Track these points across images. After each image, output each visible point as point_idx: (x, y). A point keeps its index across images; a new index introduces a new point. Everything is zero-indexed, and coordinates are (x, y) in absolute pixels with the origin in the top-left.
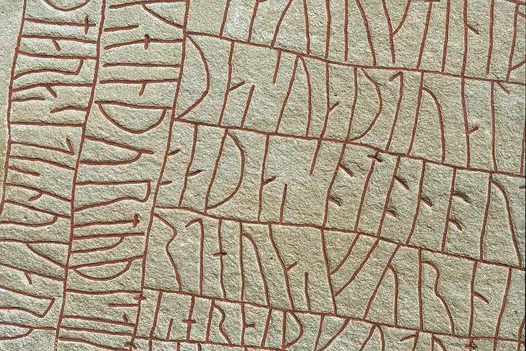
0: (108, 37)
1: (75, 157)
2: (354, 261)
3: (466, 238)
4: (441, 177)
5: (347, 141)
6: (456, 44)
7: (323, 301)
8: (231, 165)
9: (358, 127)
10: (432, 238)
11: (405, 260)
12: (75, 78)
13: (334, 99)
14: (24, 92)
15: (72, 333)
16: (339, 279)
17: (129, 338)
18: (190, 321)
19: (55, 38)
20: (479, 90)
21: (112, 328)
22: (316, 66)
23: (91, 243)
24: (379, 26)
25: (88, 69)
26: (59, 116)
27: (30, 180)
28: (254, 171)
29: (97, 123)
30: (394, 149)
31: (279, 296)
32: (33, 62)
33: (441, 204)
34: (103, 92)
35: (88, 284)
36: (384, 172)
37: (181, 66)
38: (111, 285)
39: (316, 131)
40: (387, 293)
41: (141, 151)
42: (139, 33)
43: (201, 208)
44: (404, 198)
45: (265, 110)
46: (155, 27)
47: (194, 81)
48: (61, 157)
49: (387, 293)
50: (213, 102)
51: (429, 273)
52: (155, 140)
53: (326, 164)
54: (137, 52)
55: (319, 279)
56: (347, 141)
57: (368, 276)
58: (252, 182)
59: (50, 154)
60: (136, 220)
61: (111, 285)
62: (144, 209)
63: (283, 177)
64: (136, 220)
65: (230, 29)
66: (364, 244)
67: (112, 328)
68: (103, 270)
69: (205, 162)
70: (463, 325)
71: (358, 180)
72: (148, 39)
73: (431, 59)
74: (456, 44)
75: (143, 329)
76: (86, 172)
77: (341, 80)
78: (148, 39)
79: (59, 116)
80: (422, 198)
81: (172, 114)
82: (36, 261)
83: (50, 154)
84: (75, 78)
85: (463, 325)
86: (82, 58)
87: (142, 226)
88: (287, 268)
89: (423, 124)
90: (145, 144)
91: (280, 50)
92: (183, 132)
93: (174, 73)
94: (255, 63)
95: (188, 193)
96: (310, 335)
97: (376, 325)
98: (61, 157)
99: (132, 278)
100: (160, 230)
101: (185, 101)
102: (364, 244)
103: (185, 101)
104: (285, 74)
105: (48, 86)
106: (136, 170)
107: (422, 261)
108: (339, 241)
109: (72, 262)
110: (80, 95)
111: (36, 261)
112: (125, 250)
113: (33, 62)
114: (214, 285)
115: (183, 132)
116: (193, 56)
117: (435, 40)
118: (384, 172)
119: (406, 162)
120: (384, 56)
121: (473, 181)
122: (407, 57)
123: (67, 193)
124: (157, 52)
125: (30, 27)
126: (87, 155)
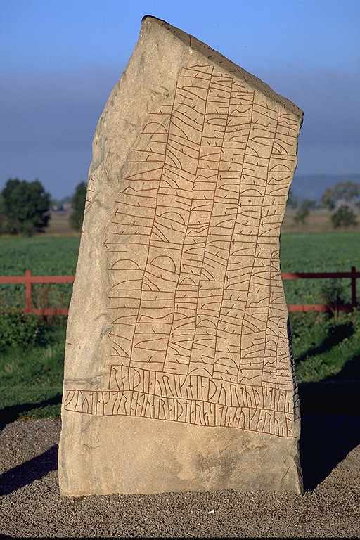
2: (251, 326)
6: (189, 300)
7: (262, 334)
8: (225, 362)
9: (213, 326)
10: (243, 304)
11: (249, 312)
13: (205, 333)
15: (276, 407)
16: (256, 330)
18: (271, 372)
19: (191, 413)
20: (202, 294)
21: (273, 395)
24: (185, 321)
25: (198, 403)
26: (213, 411)
28: (226, 355)
29: (215, 400)
32: (198, 419)
33: (233, 302)
34: (205, 399)
35: (261, 402)
40: (259, 317)
44: (232, 313)
45: (209, 352)
47: (201, 373)
48: (224, 411)
49: (259, 317)
50: (207, 367)
52: (219, 383)
54: (194, 389)
58: (229, 355)
59: (224, 414)
60: (242, 388)
65: (187, 363)
66: (245, 323)
67: (273, 395)
68: (257, 398)
70: (267, 295)
71: (227, 325)
72: (190, 386)
74: (189, 300)
75: (273, 386)
76: (229, 403)
77: (199, 331)
78: (190, 386)
79: (213, 411)
82: (255, 418)
83: (224, 414)
85: (267, 295)
88: (254, 345)
92: (216, 375)
94: (196, 355)
95: (233, 373)
96: (272, 338)
98: (224, 411)
101: (208, 375)
102: (245, 323)
103: (208, 375)
104: (198, 347)
106: (227, 388)
108: (245, 330)
111: (255, 418)
112: (250, 390)
113: (198, 419)
114: (259, 366)
115: (216, 375)
123: (235, 409)
126: (224, 404)
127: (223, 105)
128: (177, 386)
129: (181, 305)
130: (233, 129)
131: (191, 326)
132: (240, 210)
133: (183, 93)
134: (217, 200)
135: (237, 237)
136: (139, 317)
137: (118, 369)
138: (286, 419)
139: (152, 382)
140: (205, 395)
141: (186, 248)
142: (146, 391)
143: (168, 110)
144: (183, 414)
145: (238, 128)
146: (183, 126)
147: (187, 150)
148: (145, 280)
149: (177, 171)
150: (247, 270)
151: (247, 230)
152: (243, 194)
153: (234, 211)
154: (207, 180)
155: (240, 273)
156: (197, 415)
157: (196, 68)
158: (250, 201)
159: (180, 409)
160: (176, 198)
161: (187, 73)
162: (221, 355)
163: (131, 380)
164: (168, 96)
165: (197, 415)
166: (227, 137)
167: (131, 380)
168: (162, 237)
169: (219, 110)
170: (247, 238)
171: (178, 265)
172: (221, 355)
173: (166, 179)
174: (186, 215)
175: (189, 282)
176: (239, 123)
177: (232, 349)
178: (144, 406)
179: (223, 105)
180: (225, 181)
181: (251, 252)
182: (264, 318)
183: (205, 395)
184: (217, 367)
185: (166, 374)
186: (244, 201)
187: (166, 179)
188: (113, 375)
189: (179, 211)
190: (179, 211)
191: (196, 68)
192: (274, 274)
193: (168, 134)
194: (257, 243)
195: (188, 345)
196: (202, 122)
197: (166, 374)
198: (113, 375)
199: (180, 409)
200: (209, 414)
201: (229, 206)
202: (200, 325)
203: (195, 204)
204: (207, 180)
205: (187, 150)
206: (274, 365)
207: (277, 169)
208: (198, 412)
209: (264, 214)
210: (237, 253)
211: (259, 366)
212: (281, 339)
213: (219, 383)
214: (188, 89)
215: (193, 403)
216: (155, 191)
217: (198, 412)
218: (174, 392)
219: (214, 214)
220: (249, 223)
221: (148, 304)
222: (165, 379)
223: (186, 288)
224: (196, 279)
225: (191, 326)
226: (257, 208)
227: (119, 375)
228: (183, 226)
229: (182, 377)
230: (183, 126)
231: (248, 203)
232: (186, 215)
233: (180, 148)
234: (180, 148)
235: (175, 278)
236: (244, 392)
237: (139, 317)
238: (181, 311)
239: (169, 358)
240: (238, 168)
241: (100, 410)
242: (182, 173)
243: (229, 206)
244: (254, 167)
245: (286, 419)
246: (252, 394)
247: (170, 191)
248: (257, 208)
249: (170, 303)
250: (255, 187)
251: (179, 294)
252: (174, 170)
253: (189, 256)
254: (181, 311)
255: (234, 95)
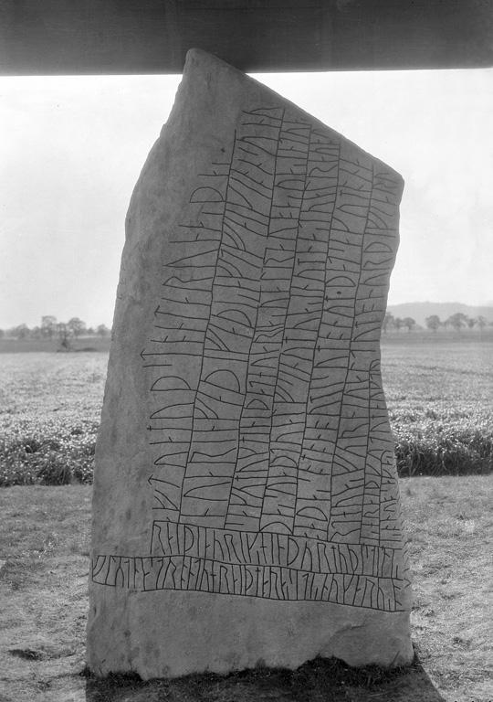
0: (262, 562)
1: (310, 574)
3: (334, 422)
4: (309, 433)
5: (297, 468)
6: (261, 430)
7: (360, 474)
9: (292, 464)
11: (343, 443)
12: (279, 575)
14: (286, 595)
16: (351, 468)
17: (380, 549)
18: (372, 525)
21: (376, 556)
22: (271, 481)
23: (344, 563)
24: (253, 459)
25: (274, 569)
27: (320, 590)
30: (300, 451)
31: (361, 490)
36: (309, 454)
37: (272, 533)
38: (360, 557)
39: (294, 480)
41: (306, 547)
42: (260, 550)
43: (327, 523)
45: (289, 500)
46: (258, 544)
47: (276, 528)
48: (310, 579)
51: (346, 435)
52: (301, 542)
53: (307, 476)
55: (352, 476)
56: (297, 468)
57: (348, 456)
59: (309, 584)
61: (360, 557)
62: (329, 545)
63: (314, 492)
64: (333, 548)
65: (258, 515)
67: (376, 556)
69: (310, 522)
73: (266, 439)
77: (273, 472)
79: (294, 581)
80: (318, 439)
81: (291, 536)
84: (279, 575)
86: (271, 572)
87: (336, 546)
89: (290, 440)
90: (304, 546)
91: (265, 496)
92: (298, 532)
93: (275, 535)
94: (270, 505)
97: (367, 453)
98: (310, 579)
99: (357, 549)
100: (338, 539)
101: (287, 531)
103: (287, 531)
105: (282, 585)
106: (313, 549)
107: (342, 437)
108: (338, 469)
109: (352, 572)
110: (285, 572)
111: (352, 589)
112: (343, 549)
113: (273, 591)
116: (268, 529)
117: (260, 438)
118: (309, 454)
119: (304, 446)
120: (266, 456)
121: (311, 420)
122: (265, 448)
124: (267, 543)
125: (260, 593)
127: (299, 162)
128: (245, 548)
129: (248, 437)
130: (313, 194)
131: (264, 465)
132: (328, 305)
133: (245, 146)
134: (294, 291)
135: (321, 343)
136: (191, 454)
137: (164, 525)
138: (394, 587)
139: (210, 541)
140: (283, 558)
141: (253, 359)
142: (202, 555)
143: (225, 170)
144: (254, 586)
145: (320, 192)
146: (245, 191)
147: (251, 224)
148: (198, 404)
149: (239, 253)
150: (340, 387)
151: (336, 332)
152: (330, 283)
153: (320, 306)
154: (280, 265)
155: (330, 390)
156: (273, 586)
157: (261, 112)
158: (339, 293)
159: (249, 580)
160: (238, 291)
161: (249, 118)
162: (305, 503)
163: (181, 541)
164: (223, 150)
165: (273, 586)
166: (306, 205)
167: (181, 541)
168: (221, 344)
169: (296, 170)
170: (338, 344)
171: (242, 381)
172: (305, 503)
173: (224, 265)
174: (252, 314)
175: (257, 404)
176: (320, 186)
177: (319, 495)
178: (200, 577)
179: (299, 162)
180: (306, 266)
181: (343, 362)
182: (363, 451)
183: (283, 558)
184: (299, 521)
185: (228, 532)
186: (331, 293)
187: (224, 265)
188: (156, 535)
189: (245, 309)
190: (245, 309)
191: (261, 112)
192: (373, 392)
193: (226, 202)
194: (351, 351)
195: (259, 491)
196: (271, 186)
197: (228, 532)
198: (156, 535)
199: (249, 576)
200: (288, 584)
201: (310, 300)
202: (275, 463)
203: (265, 298)
204: (280, 265)
205: (251, 224)
206: (376, 514)
207: (375, 248)
208: (273, 581)
209: (359, 310)
210: (325, 364)
211: (358, 517)
212: (385, 480)
213: (301, 542)
214: (251, 140)
215: (267, 569)
216: (209, 282)
217: (273, 581)
218: (241, 558)
219: (290, 312)
220: (339, 324)
221: (203, 436)
222: (228, 538)
223: (252, 413)
224: (268, 400)
225: (264, 465)
226: (351, 303)
227: (164, 535)
228: (248, 330)
229: (252, 536)
230: (245, 191)
231: (337, 296)
232: (252, 314)
233: (242, 220)
234: (242, 220)
235: (238, 399)
236: (337, 553)
237: (191, 454)
238: (249, 445)
239: (233, 510)
240: (323, 247)
241: (140, 583)
242: (246, 257)
243: (310, 300)
244: (343, 247)
245: (394, 587)
246: (347, 554)
247: (233, 282)
248: (351, 303)
249: (234, 434)
250: (346, 274)
251: (245, 422)
252: (231, 250)
253: (258, 370)
254: (249, 445)
255: (313, 148)
